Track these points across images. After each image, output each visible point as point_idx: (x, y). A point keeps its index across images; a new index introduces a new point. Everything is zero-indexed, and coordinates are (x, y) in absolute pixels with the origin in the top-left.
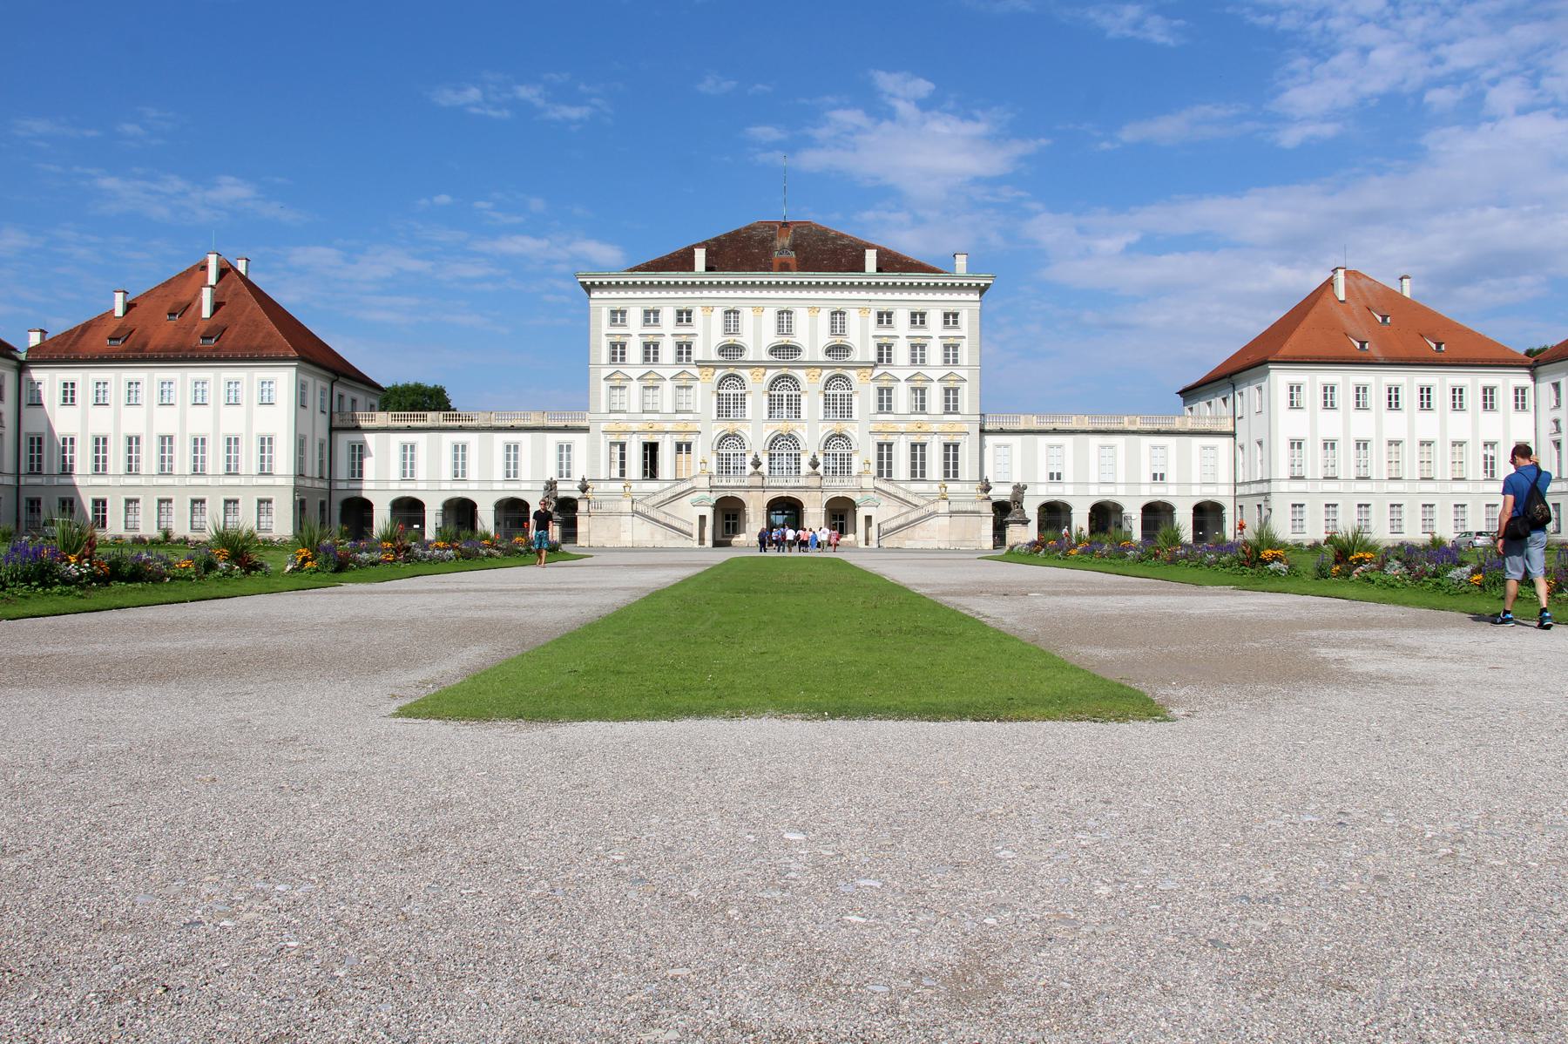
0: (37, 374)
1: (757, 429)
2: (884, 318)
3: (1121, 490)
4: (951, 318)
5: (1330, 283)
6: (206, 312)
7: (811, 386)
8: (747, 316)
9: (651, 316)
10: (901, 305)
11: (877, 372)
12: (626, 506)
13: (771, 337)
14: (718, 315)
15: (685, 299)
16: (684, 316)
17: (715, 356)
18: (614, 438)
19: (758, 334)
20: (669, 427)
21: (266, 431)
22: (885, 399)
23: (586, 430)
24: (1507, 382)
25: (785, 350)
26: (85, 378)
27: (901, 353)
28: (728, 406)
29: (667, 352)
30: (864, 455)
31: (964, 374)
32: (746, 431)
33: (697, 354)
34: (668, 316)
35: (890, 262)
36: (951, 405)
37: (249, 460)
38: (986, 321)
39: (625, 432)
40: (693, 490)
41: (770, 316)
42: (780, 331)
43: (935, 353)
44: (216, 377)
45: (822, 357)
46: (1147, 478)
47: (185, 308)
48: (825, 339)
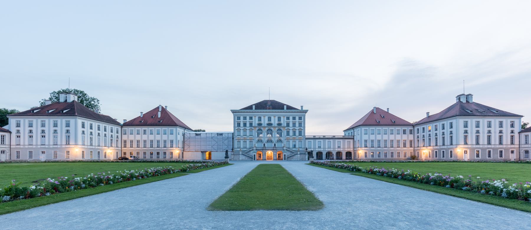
2: (288, 118)
3: (332, 149)
4: (300, 118)
6: (159, 116)
7: (275, 130)
8: (262, 118)
9: (245, 118)
11: (286, 128)
12: (241, 153)
13: (267, 122)
16: (251, 118)
19: (265, 121)
21: (172, 139)
25: (270, 124)
27: (291, 125)
29: (248, 125)
32: (262, 139)
33: (253, 125)
34: (248, 118)
35: (289, 108)
36: (300, 134)
41: (266, 118)
43: (297, 125)
47: (156, 115)
48: (277, 122)
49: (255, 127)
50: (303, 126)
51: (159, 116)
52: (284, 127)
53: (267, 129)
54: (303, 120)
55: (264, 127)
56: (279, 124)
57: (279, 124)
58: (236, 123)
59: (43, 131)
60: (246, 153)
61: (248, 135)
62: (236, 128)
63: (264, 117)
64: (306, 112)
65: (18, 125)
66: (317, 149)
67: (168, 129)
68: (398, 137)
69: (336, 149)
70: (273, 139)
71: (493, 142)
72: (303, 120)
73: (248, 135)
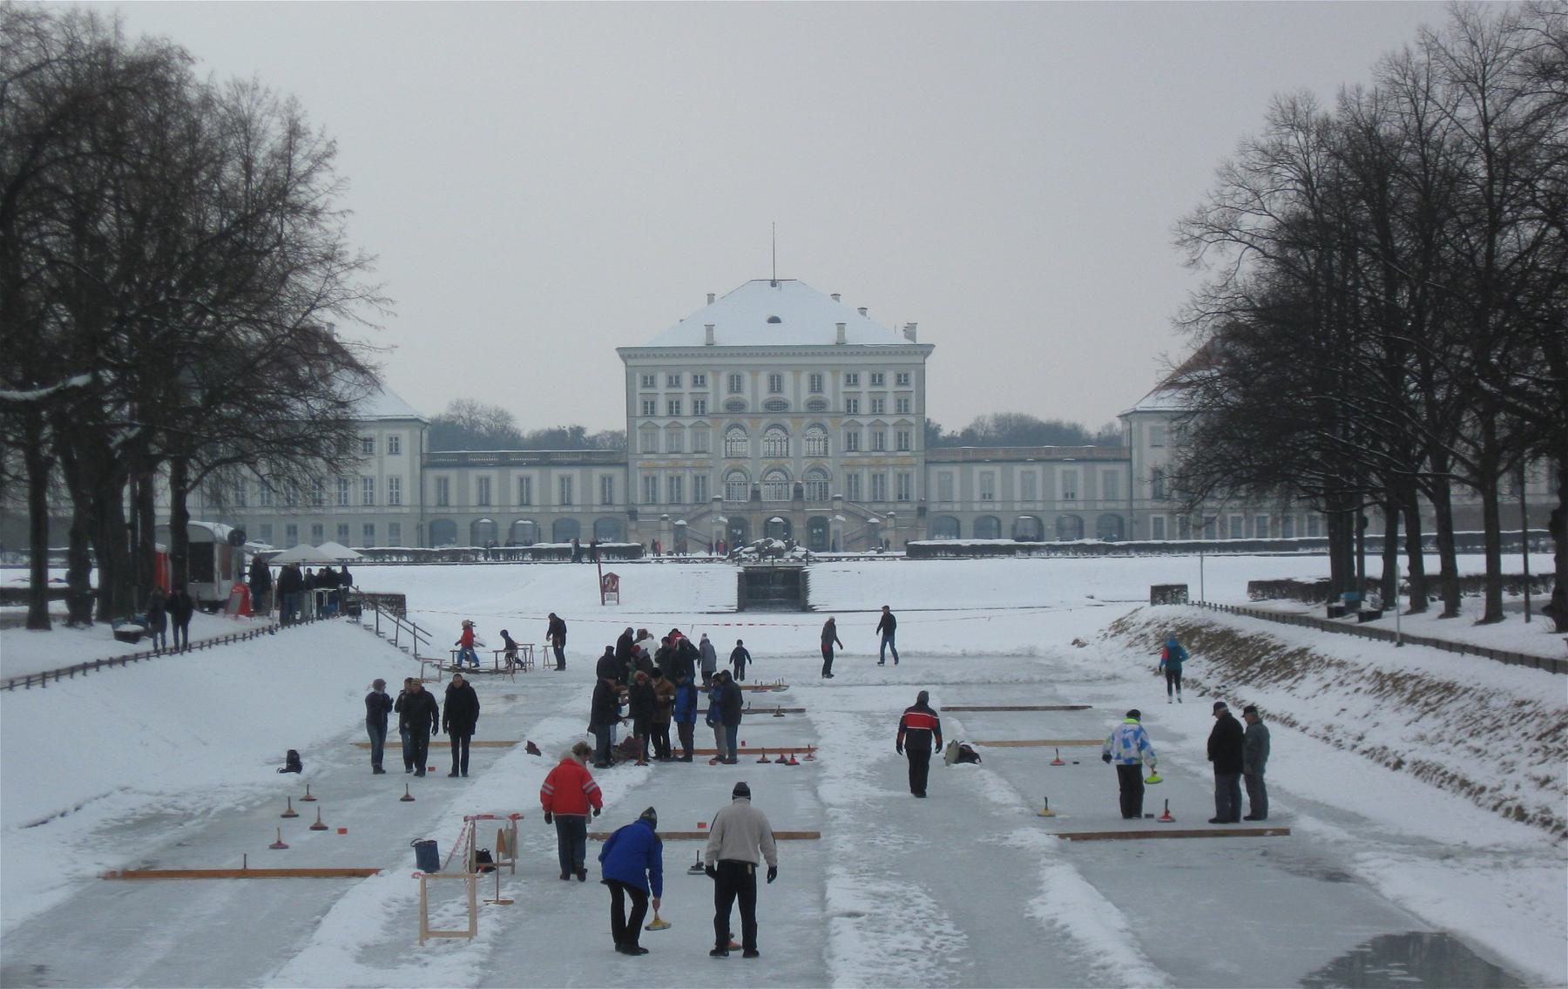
4: (902, 379)
11: (846, 420)
13: (764, 394)
14: (724, 380)
16: (699, 381)
18: (646, 473)
20: (689, 463)
22: (852, 442)
25: (777, 406)
27: (865, 406)
29: (687, 408)
30: (837, 489)
31: (912, 420)
32: (748, 466)
33: (710, 407)
37: (382, 495)
39: (657, 468)
40: (710, 512)
41: (763, 379)
42: (772, 390)
43: (890, 406)
45: (803, 408)
46: (1059, 495)
48: (806, 395)
49: (716, 416)
50: (913, 409)
52: (836, 415)
53: (765, 422)
54: (912, 387)
55: (755, 416)
56: (817, 406)
57: (817, 406)
58: (638, 398)
61: (687, 448)
62: (640, 422)
64: (927, 350)
66: (976, 507)
69: (1059, 506)
70: (790, 466)
72: (912, 387)
73: (687, 448)
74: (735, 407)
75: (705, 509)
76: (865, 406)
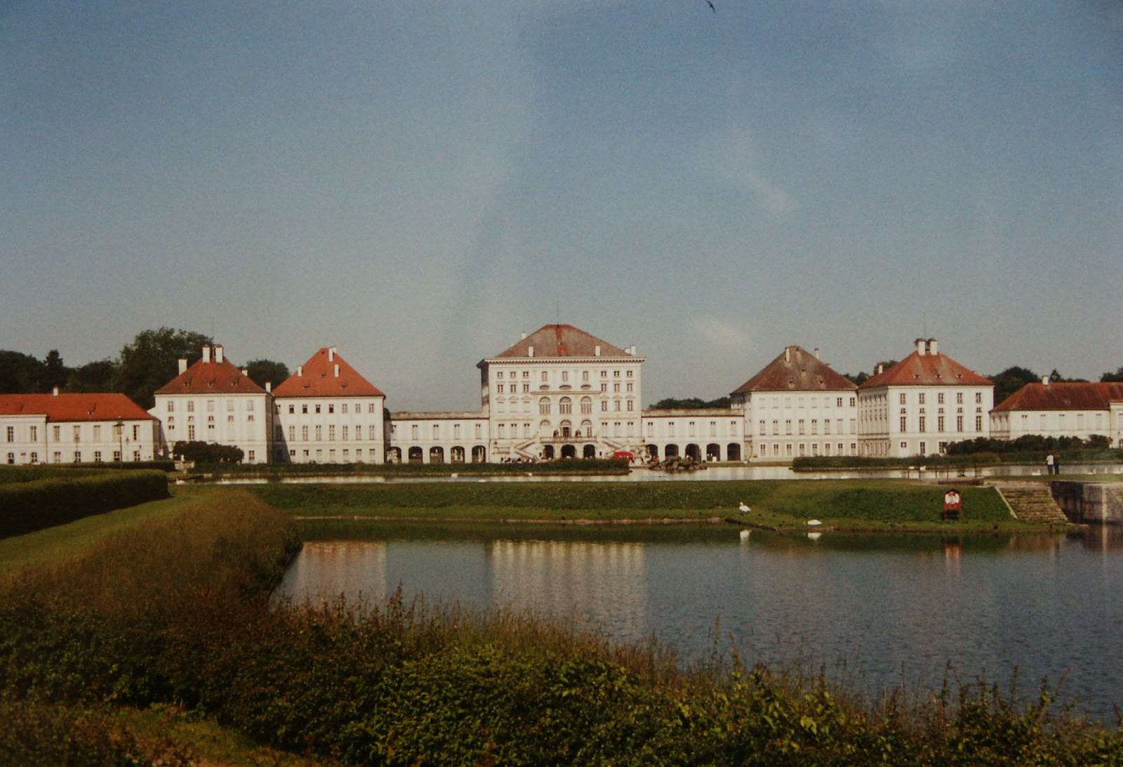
0: (277, 402)
1: (556, 419)
2: (604, 373)
4: (629, 373)
5: (785, 353)
6: (337, 375)
8: (550, 374)
10: (611, 369)
11: (601, 395)
14: (539, 375)
15: (525, 367)
16: (526, 374)
17: (539, 390)
19: (555, 381)
23: (488, 419)
24: (847, 396)
26: (298, 403)
27: (610, 387)
28: (545, 410)
29: (520, 388)
30: (597, 429)
31: (634, 395)
33: (532, 389)
36: (630, 408)
37: (365, 433)
38: (643, 374)
41: (559, 374)
43: (623, 387)
44: (352, 402)
49: (533, 393)
51: (337, 375)
59: (211, 418)
60: (522, 449)
62: (497, 396)
63: (554, 371)
65: (170, 409)
67: (365, 402)
68: (827, 414)
71: (928, 427)
74: (544, 387)
75: (531, 442)
76: (610, 387)
